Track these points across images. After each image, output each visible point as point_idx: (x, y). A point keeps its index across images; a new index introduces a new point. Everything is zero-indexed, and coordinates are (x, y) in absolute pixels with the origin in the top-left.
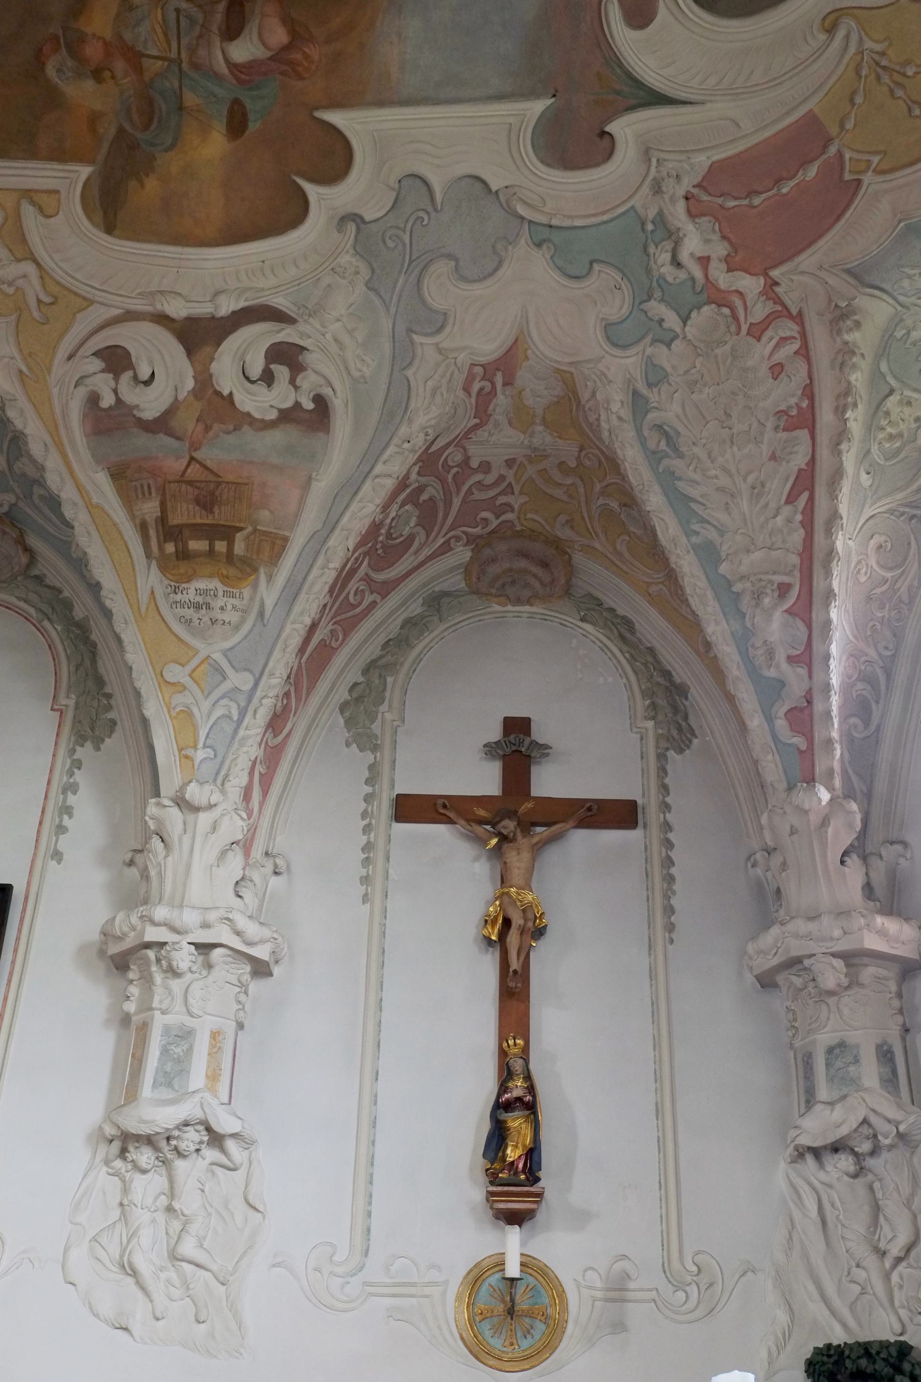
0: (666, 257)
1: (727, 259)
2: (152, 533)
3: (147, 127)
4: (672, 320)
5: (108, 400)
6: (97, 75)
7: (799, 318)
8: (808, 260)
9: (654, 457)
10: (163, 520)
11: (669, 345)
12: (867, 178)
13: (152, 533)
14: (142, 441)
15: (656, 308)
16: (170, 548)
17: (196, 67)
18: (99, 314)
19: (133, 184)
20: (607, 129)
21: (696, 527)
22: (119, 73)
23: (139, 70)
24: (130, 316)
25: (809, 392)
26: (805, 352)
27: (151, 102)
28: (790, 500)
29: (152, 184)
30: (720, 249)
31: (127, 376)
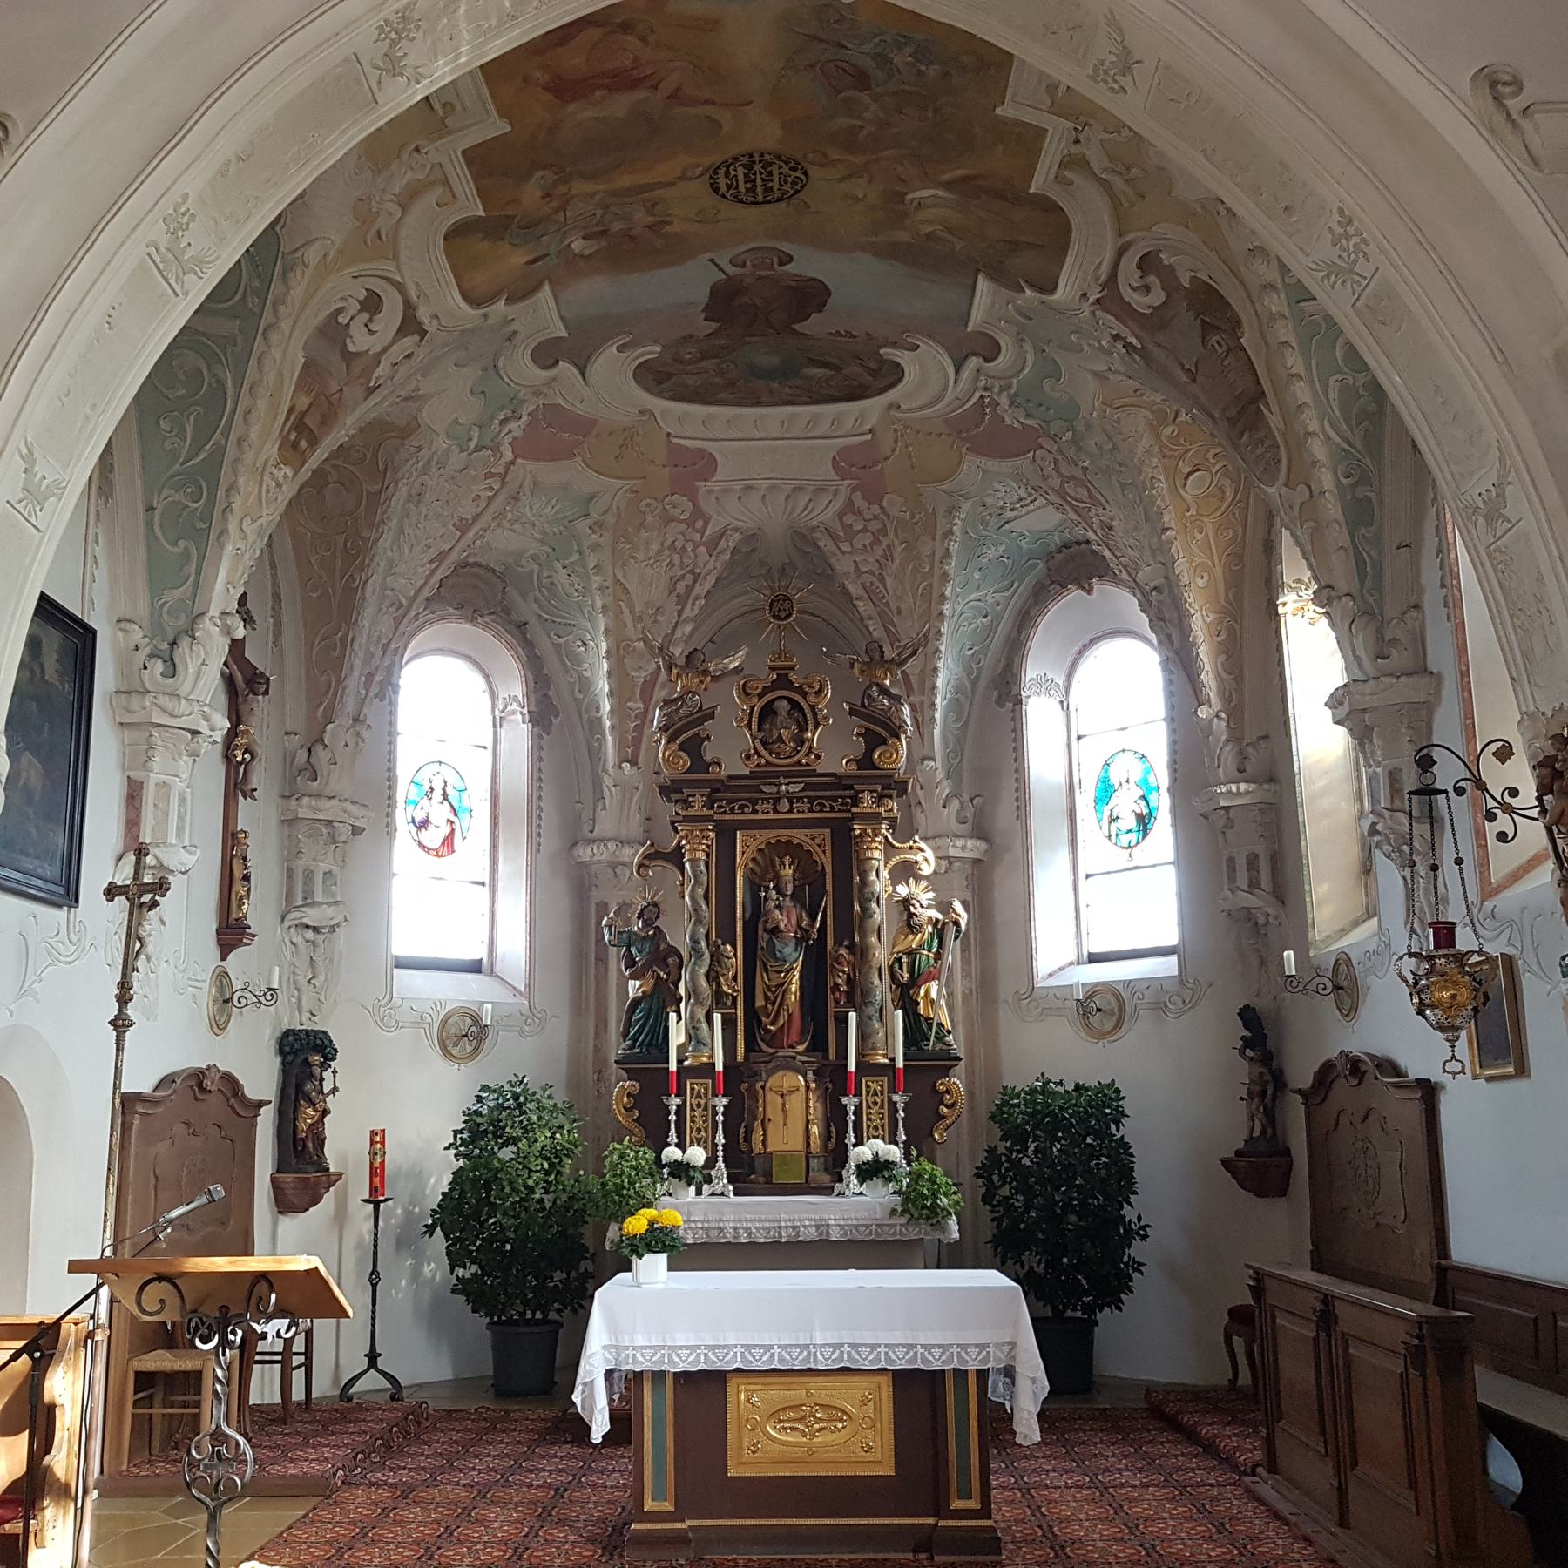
0: (502, 417)
1: (514, 438)
2: (293, 417)
3: (520, 228)
4: (472, 444)
5: (343, 320)
6: (546, 195)
7: (504, 483)
8: (532, 465)
9: (409, 498)
10: (303, 415)
11: (462, 451)
12: (578, 458)
13: (293, 417)
14: (336, 362)
15: (476, 433)
16: (293, 436)
17: (565, 233)
18: (388, 268)
19: (481, 235)
20: (561, 363)
21: (395, 548)
22: (552, 205)
23: (556, 211)
24: (399, 287)
25: (476, 518)
26: (490, 500)
27: (539, 223)
28: (431, 562)
29: (486, 244)
30: (518, 433)
31: (366, 316)
